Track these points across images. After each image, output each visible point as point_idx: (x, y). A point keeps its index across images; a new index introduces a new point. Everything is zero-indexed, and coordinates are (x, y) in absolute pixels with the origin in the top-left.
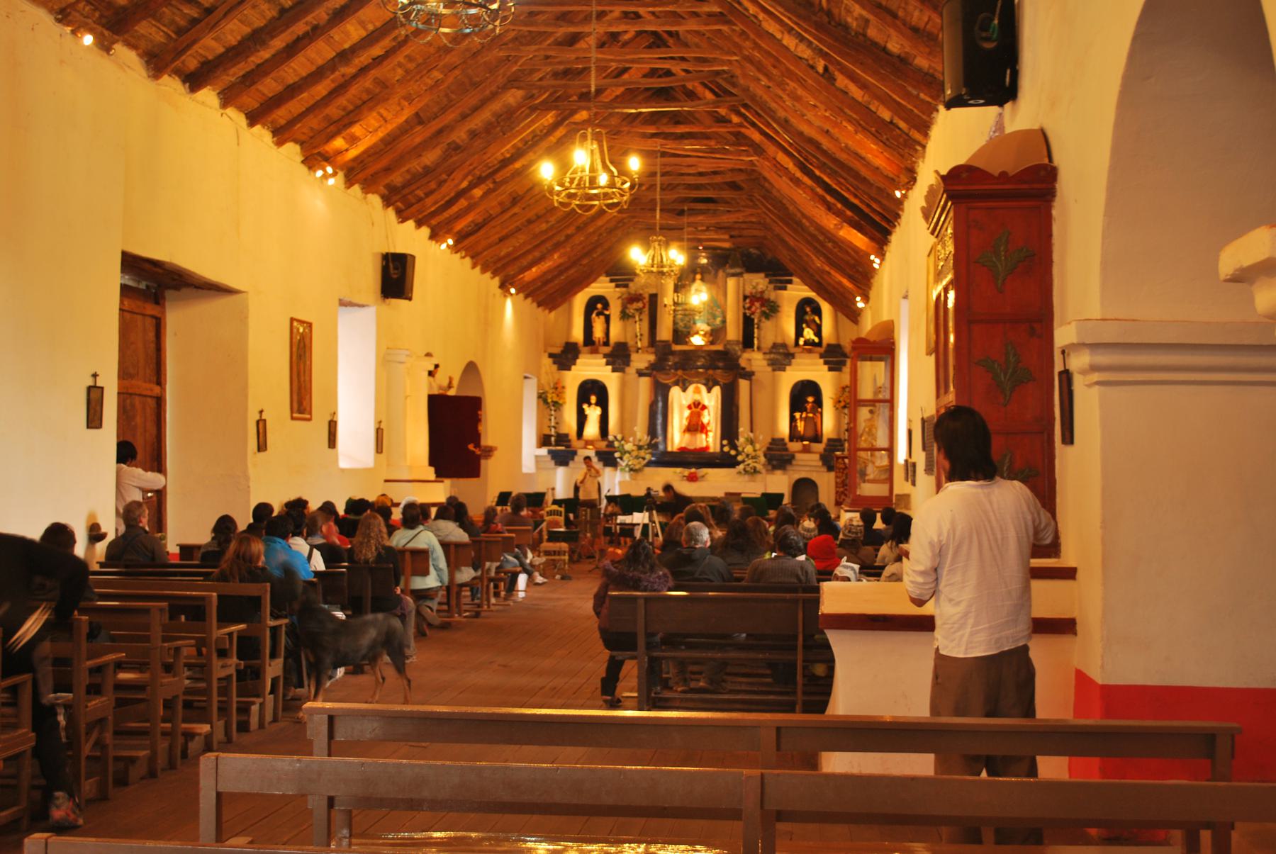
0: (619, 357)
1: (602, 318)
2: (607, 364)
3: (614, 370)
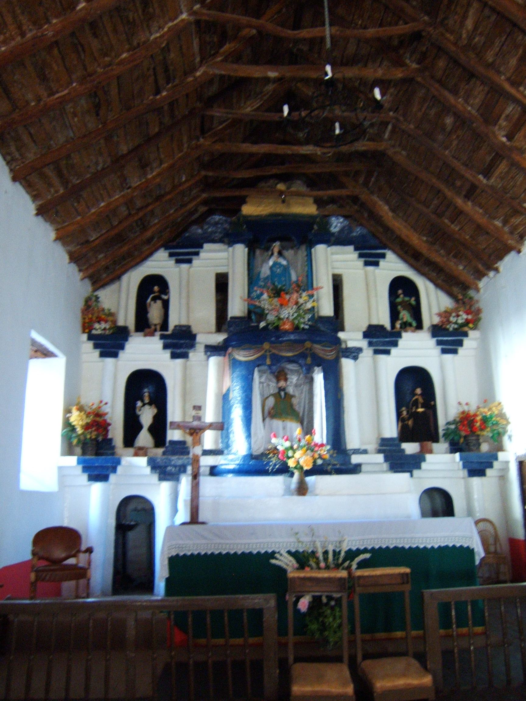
0: (180, 342)
2: (165, 347)
3: (174, 356)
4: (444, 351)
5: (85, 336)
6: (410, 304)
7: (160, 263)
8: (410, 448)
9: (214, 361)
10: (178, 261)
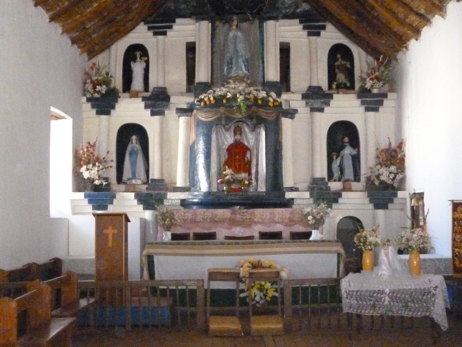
0: (158, 101)
2: (146, 107)
3: (153, 114)
4: (367, 109)
5: (84, 99)
6: (347, 68)
7: (141, 35)
9: (183, 120)
10: (155, 34)
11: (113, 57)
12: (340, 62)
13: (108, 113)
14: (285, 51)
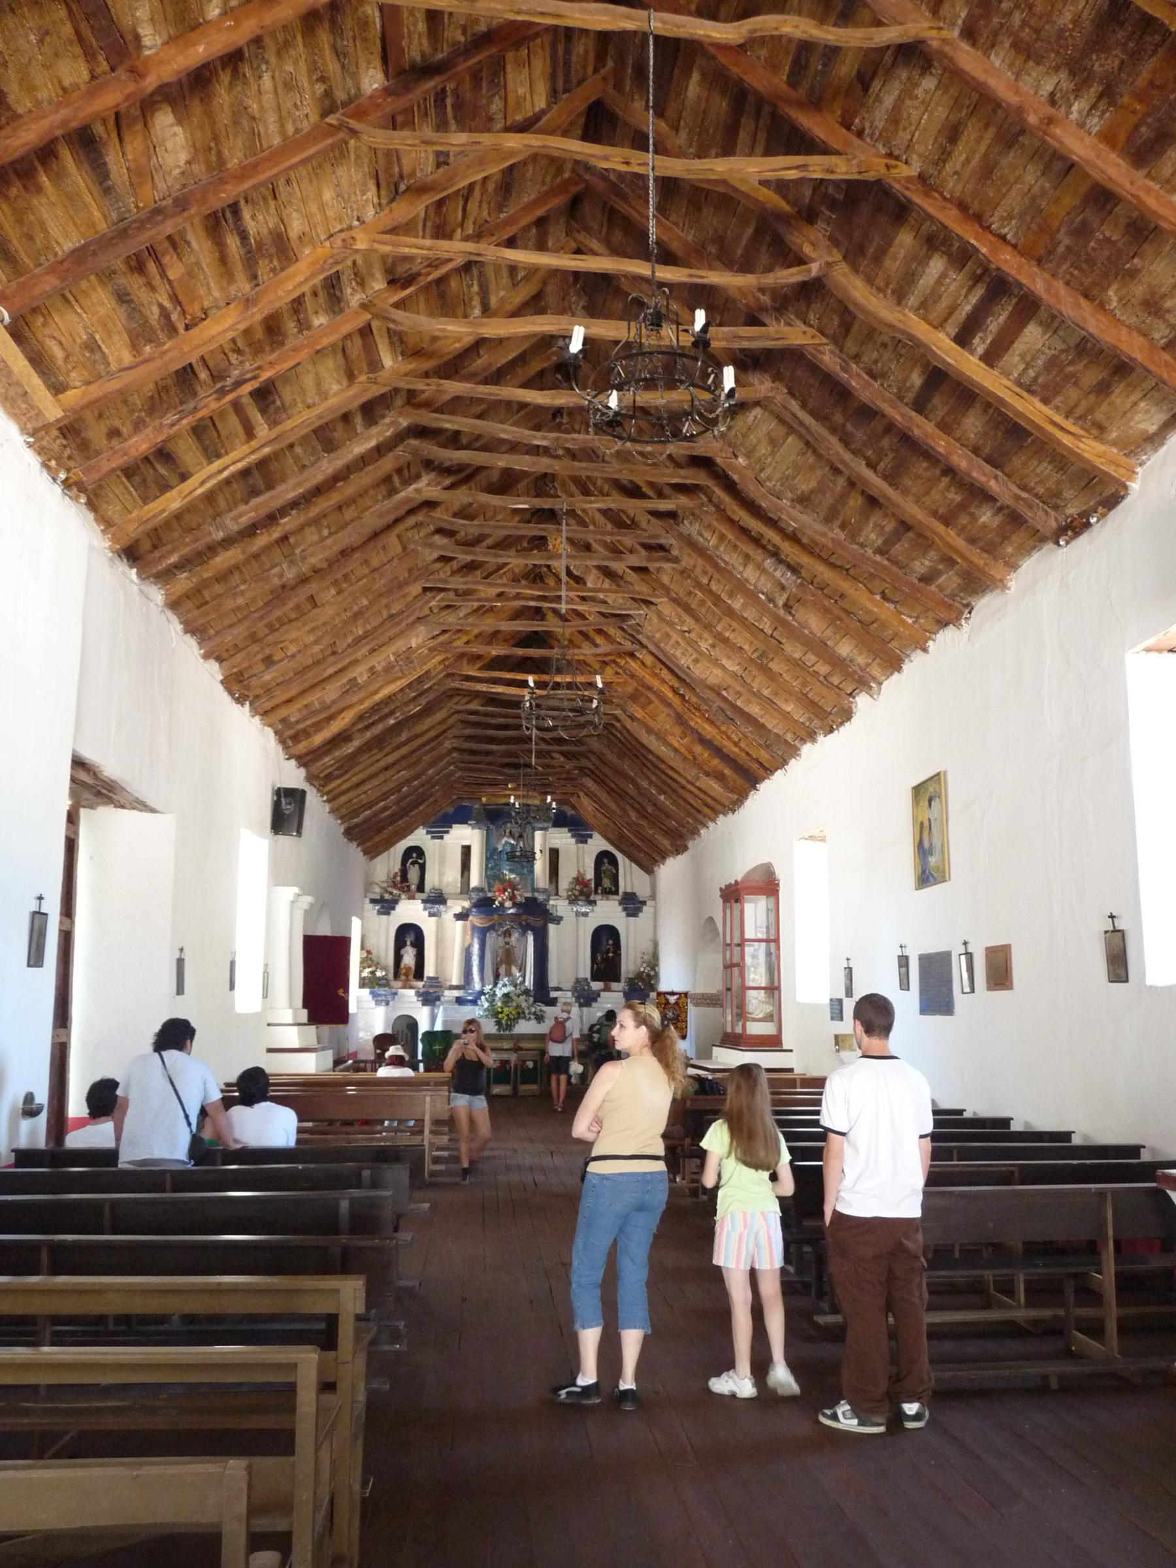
1: (417, 866)
2: (425, 909)
4: (628, 915)
5: (367, 900)
8: (596, 986)
9: (460, 923)
10: (433, 838)
11: (391, 859)
12: (606, 866)
13: (388, 914)
14: (554, 854)
